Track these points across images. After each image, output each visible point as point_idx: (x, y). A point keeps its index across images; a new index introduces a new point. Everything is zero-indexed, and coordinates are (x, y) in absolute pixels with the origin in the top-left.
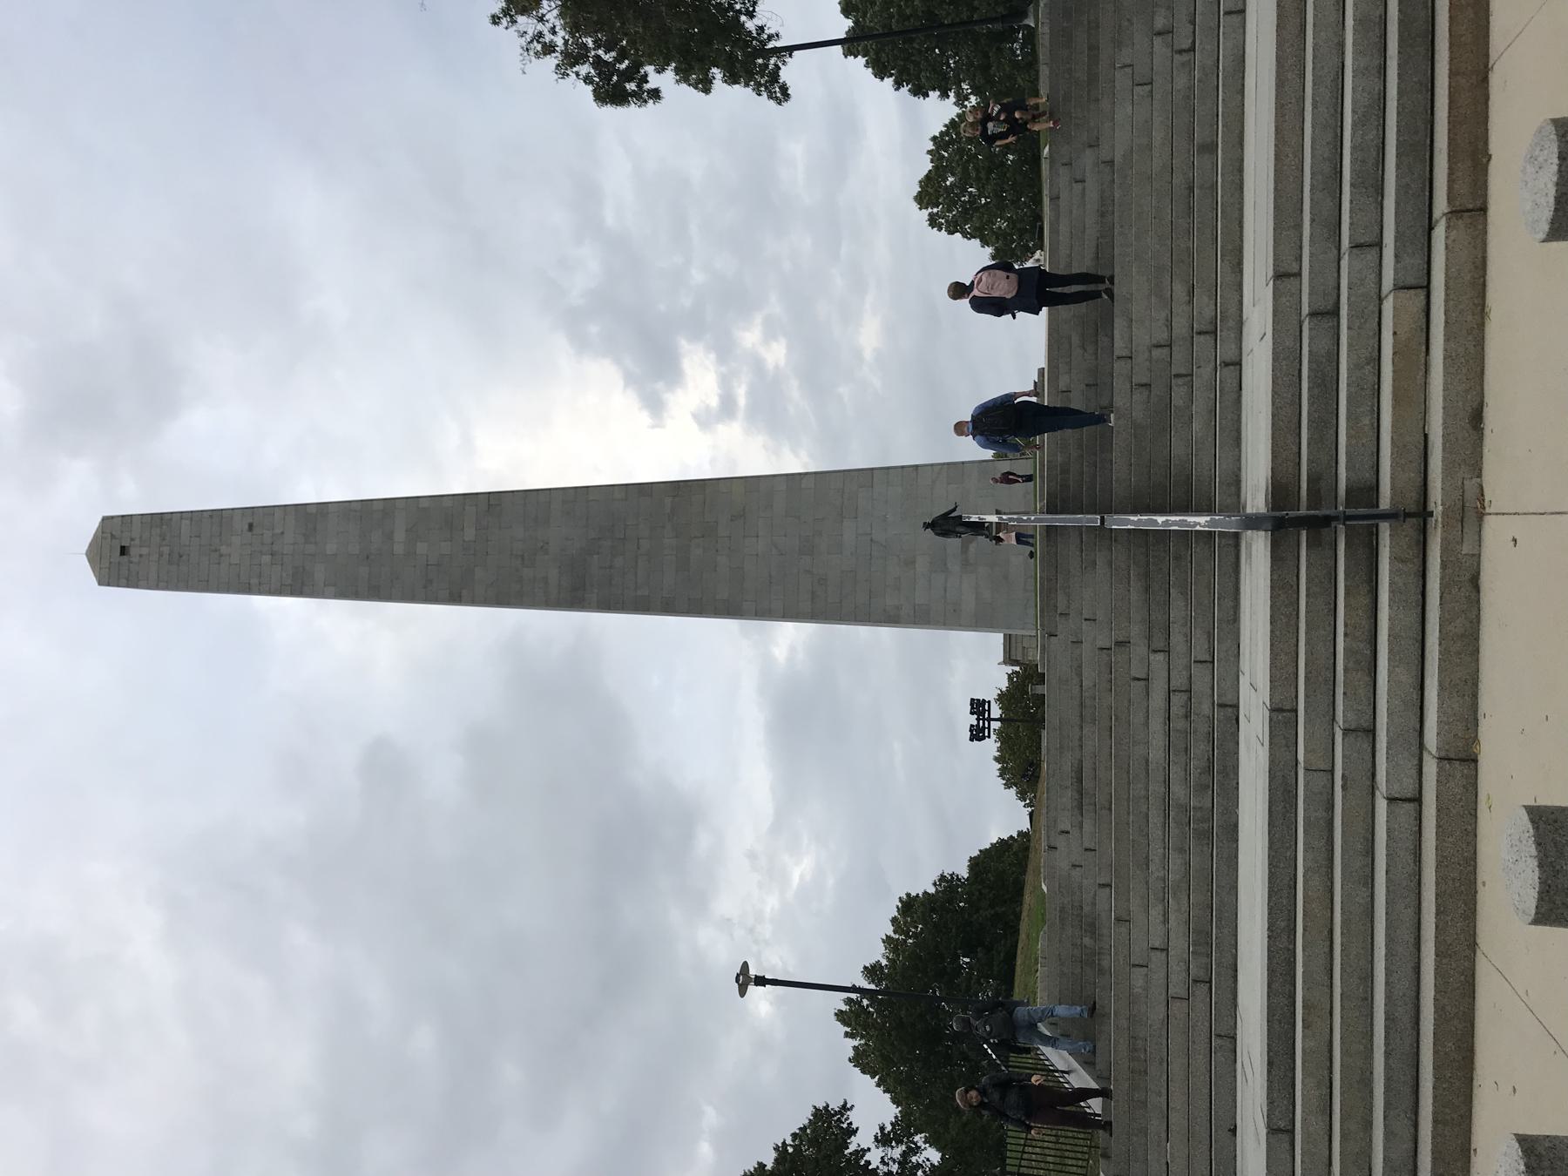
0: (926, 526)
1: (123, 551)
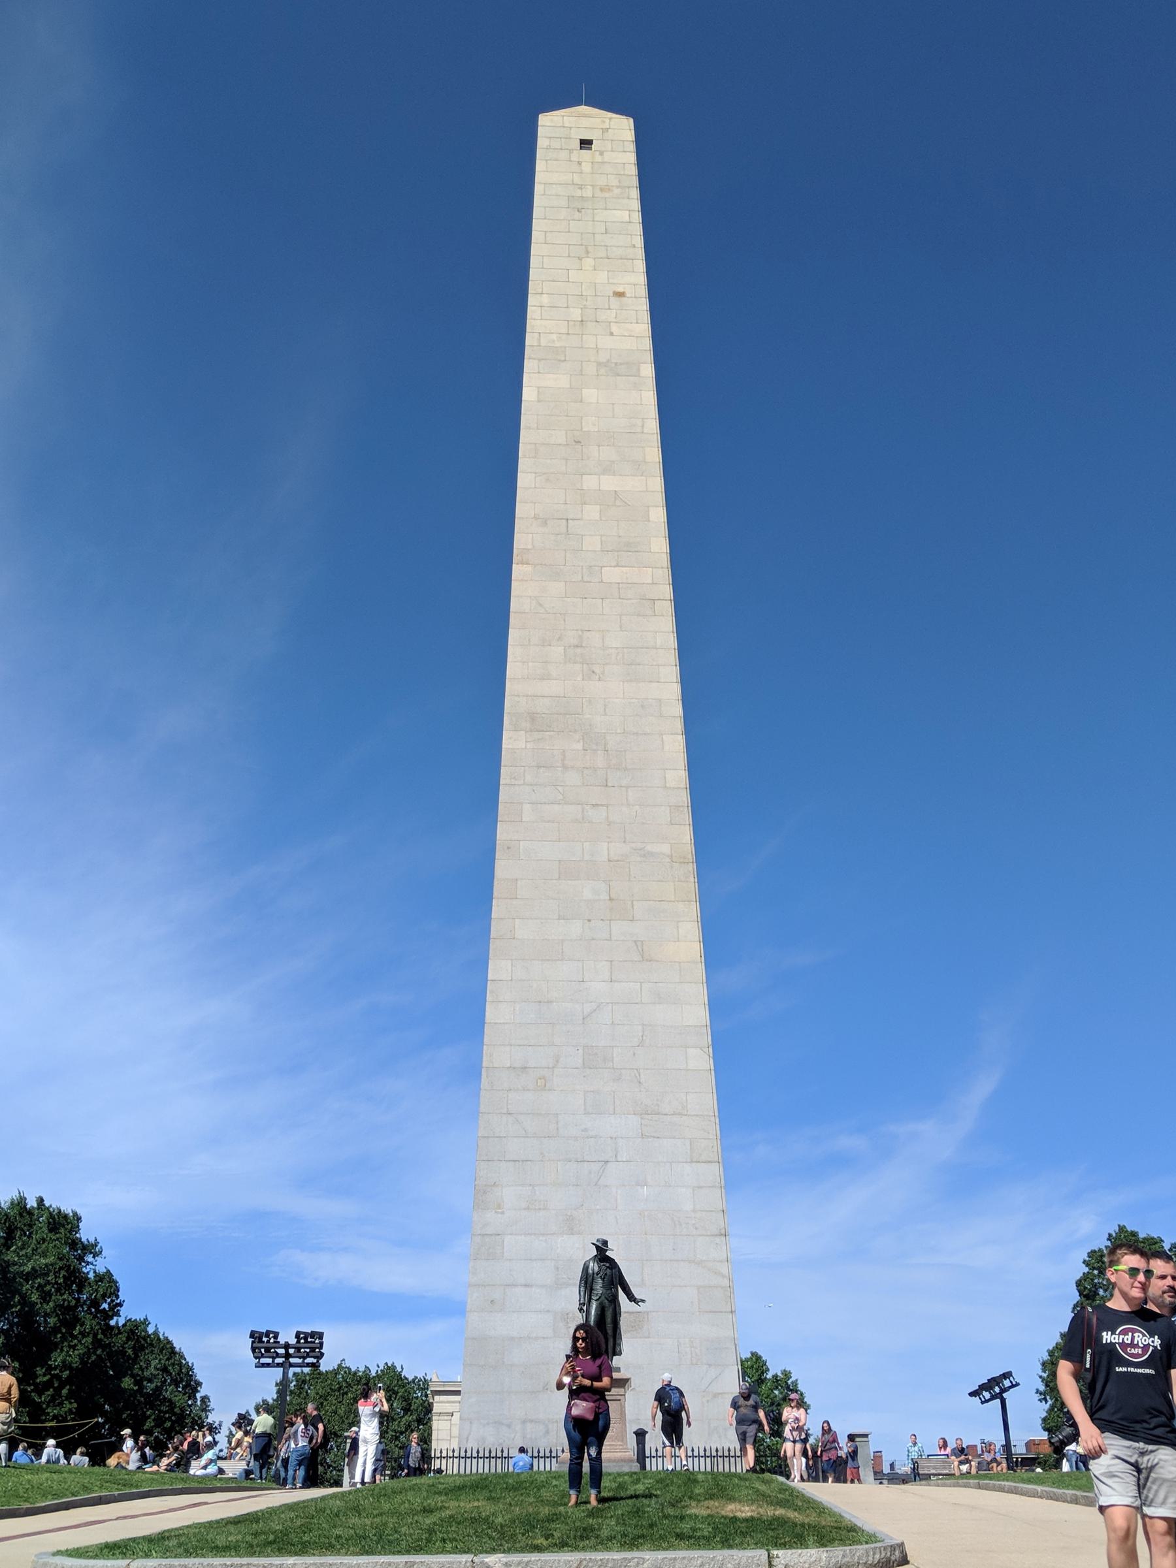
0: (602, 1250)
1: (586, 144)
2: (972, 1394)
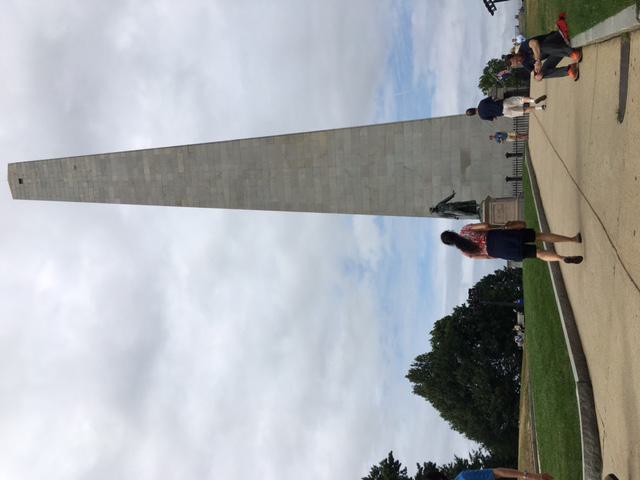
1: (21, 181)
2: (493, 14)
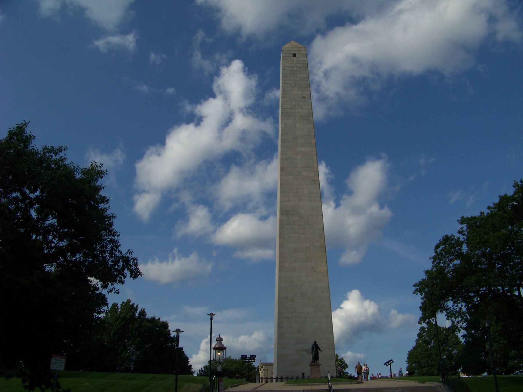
0: (315, 342)
1: (294, 55)
